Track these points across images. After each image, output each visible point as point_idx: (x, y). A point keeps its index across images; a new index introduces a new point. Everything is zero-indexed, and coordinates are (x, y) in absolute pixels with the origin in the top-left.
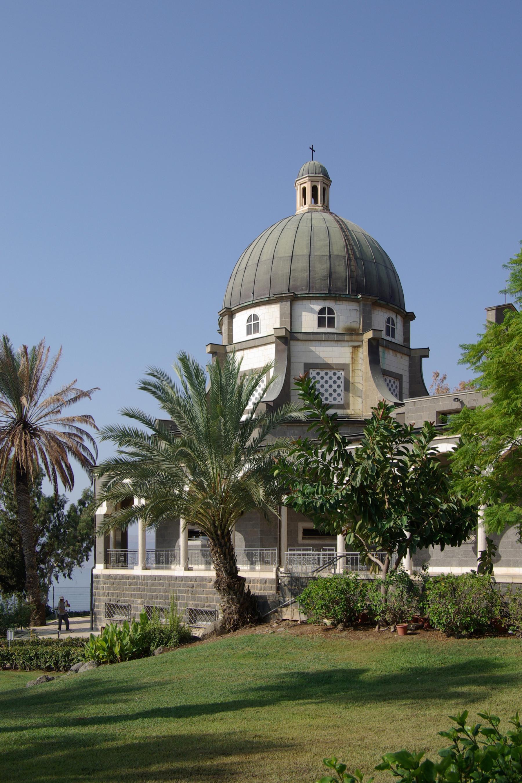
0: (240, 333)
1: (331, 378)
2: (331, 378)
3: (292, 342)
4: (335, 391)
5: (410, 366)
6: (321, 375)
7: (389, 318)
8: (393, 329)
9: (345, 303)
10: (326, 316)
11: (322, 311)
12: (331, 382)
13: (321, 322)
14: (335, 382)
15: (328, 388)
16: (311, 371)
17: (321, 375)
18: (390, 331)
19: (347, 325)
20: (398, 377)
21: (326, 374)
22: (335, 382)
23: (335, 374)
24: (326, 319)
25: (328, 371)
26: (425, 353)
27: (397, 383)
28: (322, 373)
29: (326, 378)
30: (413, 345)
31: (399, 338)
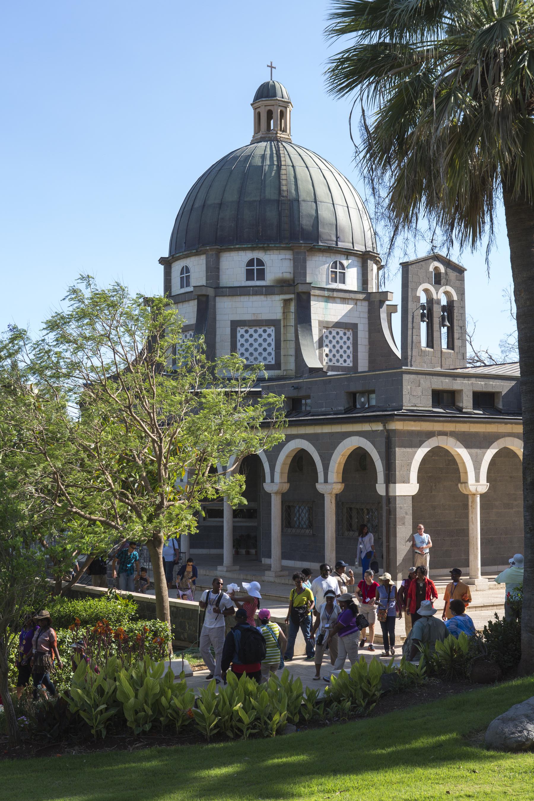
1: (260, 336)
2: (260, 336)
3: (218, 299)
4: (265, 350)
6: (249, 333)
7: (335, 263)
9: (276, 252)
10: (255, 268)
11: (250, 263)
12: (260, 340)
13: (249, 275)
14: (265, 340)
15: (258, 347)
16: (239, 329)
17: (249, 333)
19: (279, 275)
20: (353, 327)
21: (256, 331)
22: (265, 340)
23: (265, 331)
24: (256, 270)
25: (258, 329)
27: (349, 334)
28: (251, 331)
29: (256, 336)
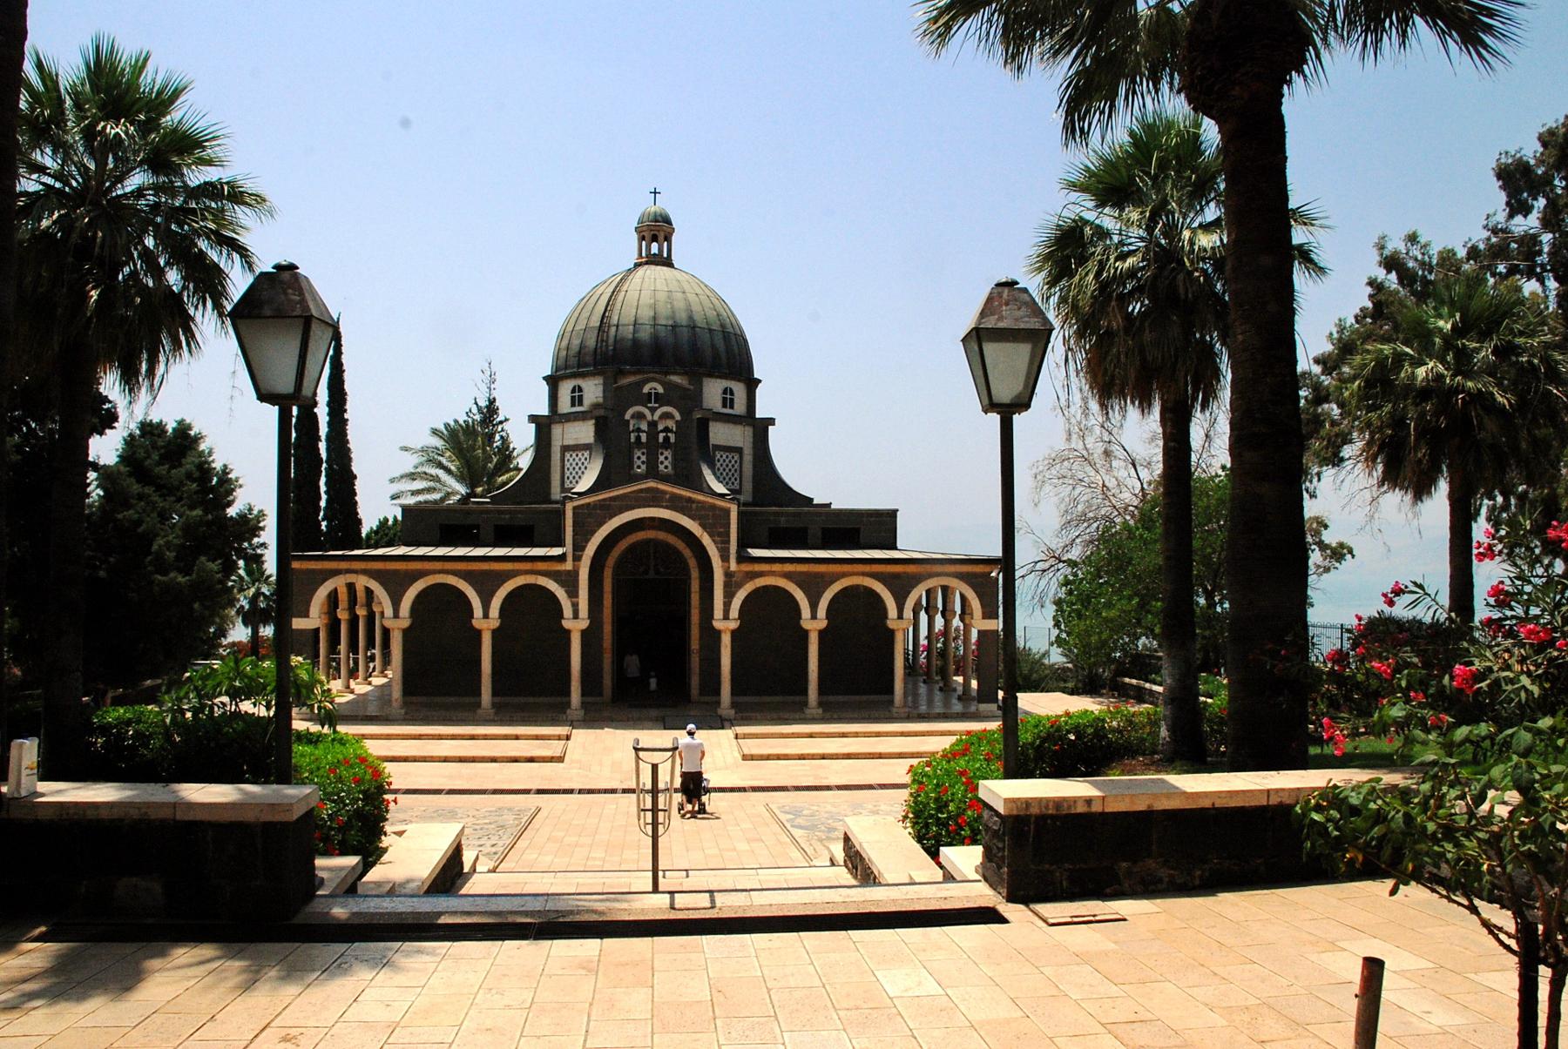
0: (565, 406)
5: (755, 435)
8: (732, 400)
18: (728, 401)
20: (739, 450)
26: (771, 421)
30: (760, 413)
31: (740, 408)
